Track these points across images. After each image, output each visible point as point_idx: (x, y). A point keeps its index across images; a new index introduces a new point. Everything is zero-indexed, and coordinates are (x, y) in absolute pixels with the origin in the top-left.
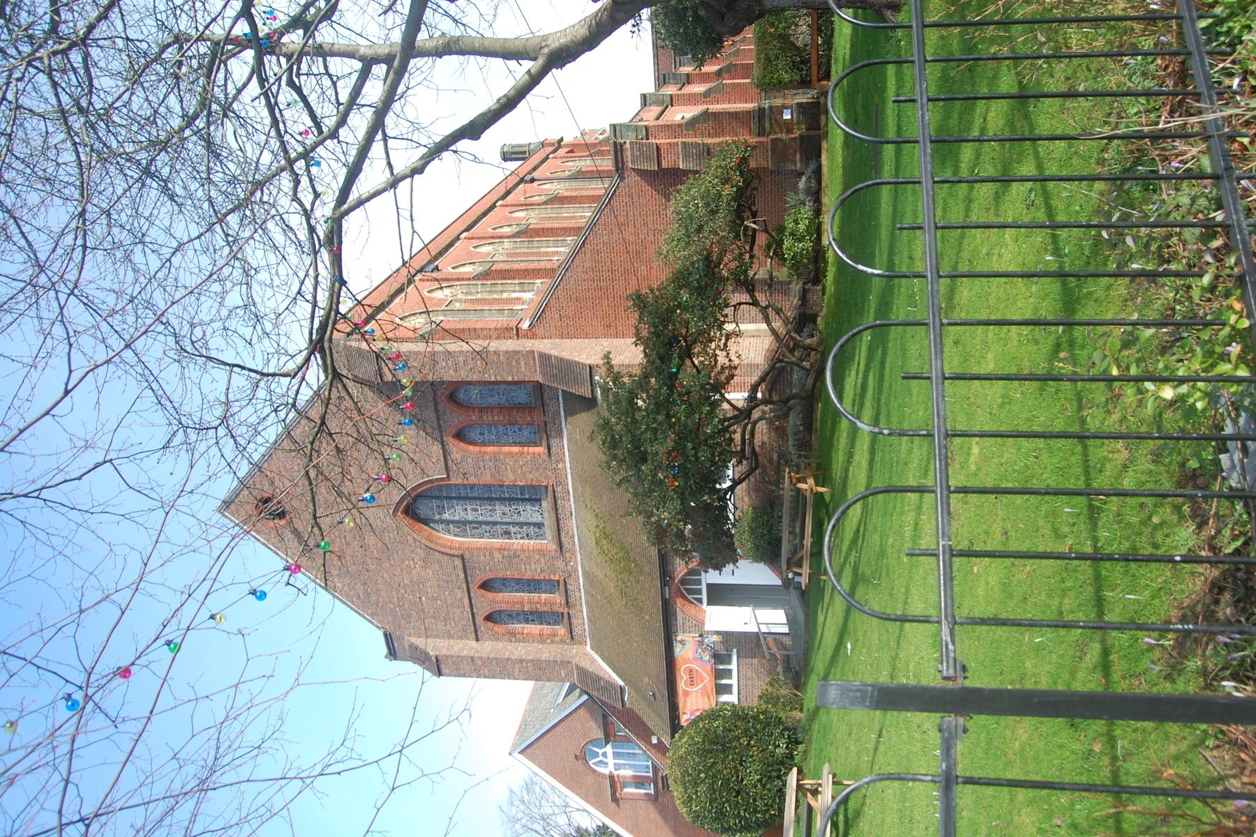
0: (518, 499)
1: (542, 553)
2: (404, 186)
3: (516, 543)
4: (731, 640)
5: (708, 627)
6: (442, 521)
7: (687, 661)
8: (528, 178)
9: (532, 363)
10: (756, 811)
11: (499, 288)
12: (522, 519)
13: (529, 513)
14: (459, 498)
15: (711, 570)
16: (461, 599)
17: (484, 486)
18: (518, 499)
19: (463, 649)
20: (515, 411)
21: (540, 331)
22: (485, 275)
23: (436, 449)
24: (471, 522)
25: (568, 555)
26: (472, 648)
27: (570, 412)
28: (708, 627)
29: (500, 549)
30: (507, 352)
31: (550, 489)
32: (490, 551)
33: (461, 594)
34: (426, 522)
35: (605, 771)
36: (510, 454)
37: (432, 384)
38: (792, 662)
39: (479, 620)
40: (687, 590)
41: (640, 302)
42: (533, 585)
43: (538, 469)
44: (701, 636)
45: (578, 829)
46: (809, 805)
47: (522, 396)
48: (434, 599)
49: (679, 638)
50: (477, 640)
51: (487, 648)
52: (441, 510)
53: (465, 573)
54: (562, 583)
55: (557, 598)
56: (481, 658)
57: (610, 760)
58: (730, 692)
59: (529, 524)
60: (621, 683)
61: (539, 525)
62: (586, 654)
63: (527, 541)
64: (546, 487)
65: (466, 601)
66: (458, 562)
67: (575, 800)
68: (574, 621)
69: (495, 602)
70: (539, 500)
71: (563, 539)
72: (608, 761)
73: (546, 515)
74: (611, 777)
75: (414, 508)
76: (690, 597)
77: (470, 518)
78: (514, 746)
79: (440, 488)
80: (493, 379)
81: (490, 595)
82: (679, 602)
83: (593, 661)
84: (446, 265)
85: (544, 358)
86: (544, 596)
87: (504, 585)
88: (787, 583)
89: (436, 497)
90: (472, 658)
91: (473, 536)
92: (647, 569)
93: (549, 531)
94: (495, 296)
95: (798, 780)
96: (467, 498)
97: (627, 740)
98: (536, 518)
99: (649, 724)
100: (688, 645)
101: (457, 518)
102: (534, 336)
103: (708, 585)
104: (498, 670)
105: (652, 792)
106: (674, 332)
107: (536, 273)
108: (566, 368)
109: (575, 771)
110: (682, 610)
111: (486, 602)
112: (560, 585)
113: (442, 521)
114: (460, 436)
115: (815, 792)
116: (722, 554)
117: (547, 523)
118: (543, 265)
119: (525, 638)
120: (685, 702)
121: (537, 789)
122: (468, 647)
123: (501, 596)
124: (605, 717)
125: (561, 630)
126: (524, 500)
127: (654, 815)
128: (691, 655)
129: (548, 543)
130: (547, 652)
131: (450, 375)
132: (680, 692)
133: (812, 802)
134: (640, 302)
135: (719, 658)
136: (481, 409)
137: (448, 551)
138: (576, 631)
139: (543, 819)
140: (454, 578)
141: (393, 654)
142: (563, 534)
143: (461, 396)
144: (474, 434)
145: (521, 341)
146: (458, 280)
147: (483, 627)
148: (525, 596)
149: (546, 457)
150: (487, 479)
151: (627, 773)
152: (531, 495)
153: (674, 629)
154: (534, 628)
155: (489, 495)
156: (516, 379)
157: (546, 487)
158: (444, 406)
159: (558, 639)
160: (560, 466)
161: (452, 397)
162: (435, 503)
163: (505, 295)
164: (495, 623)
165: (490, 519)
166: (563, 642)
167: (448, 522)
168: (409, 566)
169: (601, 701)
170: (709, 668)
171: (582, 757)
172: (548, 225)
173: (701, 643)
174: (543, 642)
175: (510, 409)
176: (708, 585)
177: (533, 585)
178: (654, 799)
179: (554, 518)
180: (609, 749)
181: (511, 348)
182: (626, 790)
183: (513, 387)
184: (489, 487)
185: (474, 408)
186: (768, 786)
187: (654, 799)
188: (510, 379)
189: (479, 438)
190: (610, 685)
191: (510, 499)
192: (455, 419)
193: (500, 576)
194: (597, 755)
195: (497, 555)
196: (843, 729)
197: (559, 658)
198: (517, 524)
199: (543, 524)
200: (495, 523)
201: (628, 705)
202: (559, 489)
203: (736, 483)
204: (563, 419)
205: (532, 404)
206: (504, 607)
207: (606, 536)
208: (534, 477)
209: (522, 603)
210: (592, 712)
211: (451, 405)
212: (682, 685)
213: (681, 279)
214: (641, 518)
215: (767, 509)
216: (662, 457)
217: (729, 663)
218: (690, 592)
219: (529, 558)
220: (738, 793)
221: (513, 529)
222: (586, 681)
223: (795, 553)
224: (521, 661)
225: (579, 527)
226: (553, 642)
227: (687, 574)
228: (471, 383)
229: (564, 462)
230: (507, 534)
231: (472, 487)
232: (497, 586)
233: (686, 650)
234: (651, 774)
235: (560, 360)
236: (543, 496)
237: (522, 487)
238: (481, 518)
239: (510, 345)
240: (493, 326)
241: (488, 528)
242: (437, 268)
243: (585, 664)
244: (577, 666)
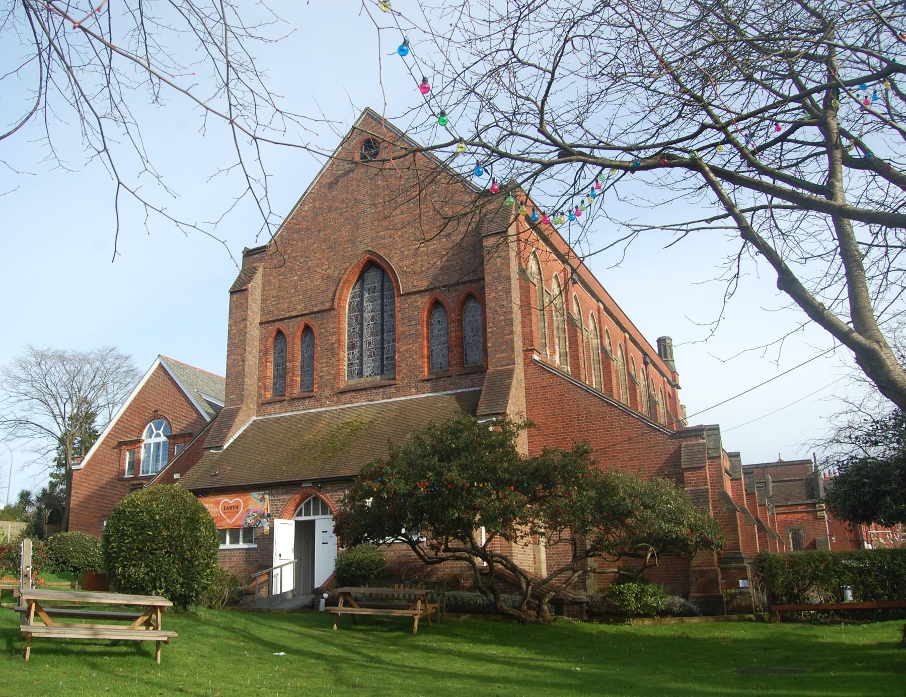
1: (337, 376)
2: (731, 221)
3: (345, 355)
4: (268, 540)
5: (277, 522)
6: (362, 292)
7: (246, 503)
8: (649, 361)
9: (504, 363)
10: (124, 566)
11: (562, 335)
12: (365, 359)
13: (369, 365)
14: (382, 305)
15: (334, 523)
16: (296, 309)
17: (394, 326)
19: (253, 312)
20: (460, 350)
21: (531, 369)
22: (571, 321)
23: (424, 284)
24: (362, 315)
25: (335, 399)
26: (254, 319)
27: (459, 397)
28: (277, 522)
29: (339, 341)
30: (513, 341)
31: (393, 382)
32: (339, 333)
33: (300, 308)
34: (361, 278)
35: (143, 437)
36: (422, 347)
37: (483, 279)
38: (246, 596)
39: (278, 325)
40: (309, 502)
41: (582, 453)
42: (308, 368)
44: (269, 515)
45: (94, 415)
46: (137, 618)
47: (474, 356)
48: (295, 287)
49: (267, 496)
50: (260, 324)
51: (254, 332)
52: (372, 291)
53: (318, 312)
54: (311, 394)
55: (297, 391)
56: (246, 327)
57: (154, 440)
58: (231, 543)
59: (361, 365)
60: (225, 447)
61: (360, 374)
62: (249, 416)
63: (346, 363)
64: (394, 379)
65: (294, 313)
66: (327, 305)
67: (119, 412)
68: (277, 406)
69: (294, 337)
70: (382, 373)
71: (349, 395)
72: (153, 438)
73: (370, 379)
74: (139, 441)
75: (373, 266)
76: (303, 505)
77: (365, 315)
78: (166, 359)
79: (391, 289)
80: (489, 330)
81: (299, 334)
82: (297, 497)
83: (243, 422)
84: (577, 290)
85: (510, 374)
86: (299, 379)
87: (308, 346)
88: (318, 592)
89: (382, 286)
90: (246, 319)
91: (350, 318)
92: (327, 467)
93: (355, 382)
94: (555, 332)
95: (161, 607)
96: (383, 311)
97: (171, 455)
98: (367, 371)
99: (190, 471)
100: (260, 504)
101: (365, 304)
102: (526, 364)
103: (313, 522)
104: (236, 341)
105: (126, 476)
106: (542, 485)
107: (576, 366)
108: (502, 393)
109: (143, 411)
110: (290, 499)
111: (293, 330)
112: (308, 394)
113: (362, 292)
114: (436, 304)
115: (147, 624)
116: (347, 531)
117: (363, 380)
118: (582, 371)
119: (262, 364)
120: (210, 503)
121: (128, 380)
122: (255, 315)
123: (298, 342)
124: (191, 435)
125: (269, 395)
127: (107, 478)
128: (252, 507)
129: (345, 381)
130: (251, 383)
131: (490, 295)
132: (219, 498)
133: (139, 621)
134: (582, 453)
135: (248, 532)
136: (460, 322)
137: (337, 297)
138: (269, 408)
139: (104, 384)
140: (314, 303)
141: (248, 254)
142: (353, 394)
143: (471, 304)
144: (438, 315)
145: (522, 354)
146: (567, 300)
147: (272, 328)
148: (298, 364)
149: (421, 377)
150: (400, 328)
151: (142, 455)
152: (387, 365)
153: (274, 492)
154: (270, 373)
155: (386, 329)
156: (489, 350)
157: (394, 379)
158: (463, 290)
159: (262, 392)
160: (413, 390)
161: (470, 296)
162: (378, 285)
163: (556, 340)
164: (275, 338)
165: (365, 331)
166: (260, 396)
167: (362, 297)
168: (323, 264)
169: (209, 430)
170: (240, 523)
171: (156, 416)
172: (614, 376)
173: (262, 516)
174: (259, 379)
175: (461, 345)
176: (313, 522)
177: (308, 368)
178: (120, 478)
179: (367, 386)
180: (163, 439)
181: (516, 345)
182: (128, 454)
183: (481, 348)
184: (393, 330)
185: (461, 315)
186: (146, 578)
187: (120, 478)
188: (489, 345)
189: (434, 321)
190: (224, 438)
191: (382, 348)
192: (450, 299)
193: (317, 341)
194: (158, 428)
195: (334, 338)
196: (206, 650)
197: (246, 393)
198: (361, 355)
199: (362, 377)
200: (361, 336)
201: (206, 453)
202: (393, 390)
203: (413, 544)
204: (455, 391)
205: (468, 362)
206: (290, 345)
207: (354, 431)
208: (403, 368)
209: (293, 361)
210: (194, 424)
211: (464, 293)
212: (225, 500)
213: (607, 489)
214: (386, 458)
215: (389, 574)
216: (448, 475)
217: (244, 542)
218: (307, 506)
219: (333, 366)
220: (141, 550)
221: (356, 351)
222: (223, 418)
223: (356, 600)
224: (243, 361)
225: (360, 407)
226: (259, 387)
227: (323, 503)
228: (484, 312)
229: (416, 393)
230: (352, 347)
231: (393, 316)
232: (308, 339)
233: (257, 503)
234: (141, 475)
235: (508, 387)
236: (384, 377)
237: (393, 358)
238: (365, 324)
239: (519, 344)
240: (533, 329)
241: (357, 330)
242: (575, 283)
243: (241, 416)
244: (239, 409)
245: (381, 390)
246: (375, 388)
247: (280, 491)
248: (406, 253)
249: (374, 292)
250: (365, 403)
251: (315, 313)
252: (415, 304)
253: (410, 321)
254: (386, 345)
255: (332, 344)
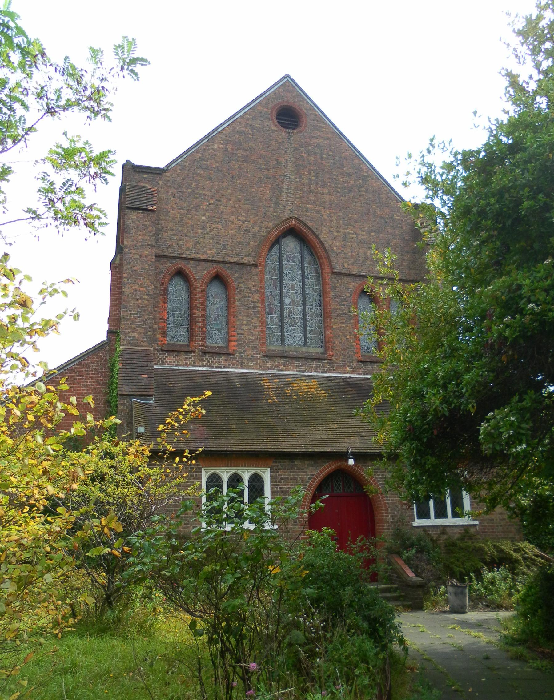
0: (305, 326)
18: (305, 326)
33: (210, 253)
43: (343, 349)
48: (204, 228)
65: (203, 257)
66: (250, 260)
68: (182, 357)
71: (276, 360)
126: (305, 331)
142: (281, 361)
160: (348, 368)
168: (240, 215)
245: (314, 362)
246: (307, 359)
247: (306, 462)
248: (335, 234)
249: (294, 262)
250: (295, 373)
251: (230, 263)
252: (347, 286)
253: (342, 301)
254: (309, 318)
255: (254, 302)
